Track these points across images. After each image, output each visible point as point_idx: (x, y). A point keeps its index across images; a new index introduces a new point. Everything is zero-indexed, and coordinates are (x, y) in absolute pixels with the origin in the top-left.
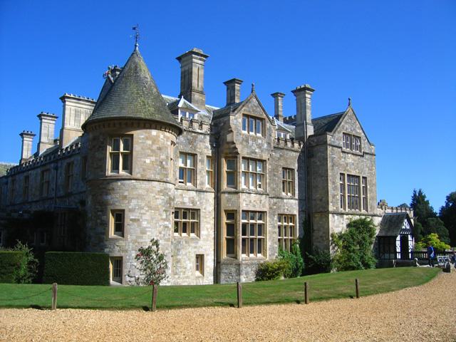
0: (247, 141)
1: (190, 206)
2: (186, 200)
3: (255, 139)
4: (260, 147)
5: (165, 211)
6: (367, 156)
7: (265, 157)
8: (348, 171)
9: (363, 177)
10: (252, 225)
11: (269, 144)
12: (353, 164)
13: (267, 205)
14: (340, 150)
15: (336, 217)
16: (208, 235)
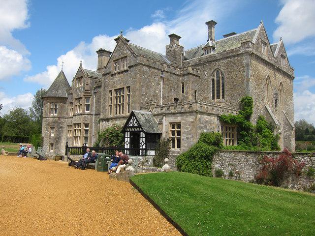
4: (80, 91)
9: (127, 87)
10: (78, 130)
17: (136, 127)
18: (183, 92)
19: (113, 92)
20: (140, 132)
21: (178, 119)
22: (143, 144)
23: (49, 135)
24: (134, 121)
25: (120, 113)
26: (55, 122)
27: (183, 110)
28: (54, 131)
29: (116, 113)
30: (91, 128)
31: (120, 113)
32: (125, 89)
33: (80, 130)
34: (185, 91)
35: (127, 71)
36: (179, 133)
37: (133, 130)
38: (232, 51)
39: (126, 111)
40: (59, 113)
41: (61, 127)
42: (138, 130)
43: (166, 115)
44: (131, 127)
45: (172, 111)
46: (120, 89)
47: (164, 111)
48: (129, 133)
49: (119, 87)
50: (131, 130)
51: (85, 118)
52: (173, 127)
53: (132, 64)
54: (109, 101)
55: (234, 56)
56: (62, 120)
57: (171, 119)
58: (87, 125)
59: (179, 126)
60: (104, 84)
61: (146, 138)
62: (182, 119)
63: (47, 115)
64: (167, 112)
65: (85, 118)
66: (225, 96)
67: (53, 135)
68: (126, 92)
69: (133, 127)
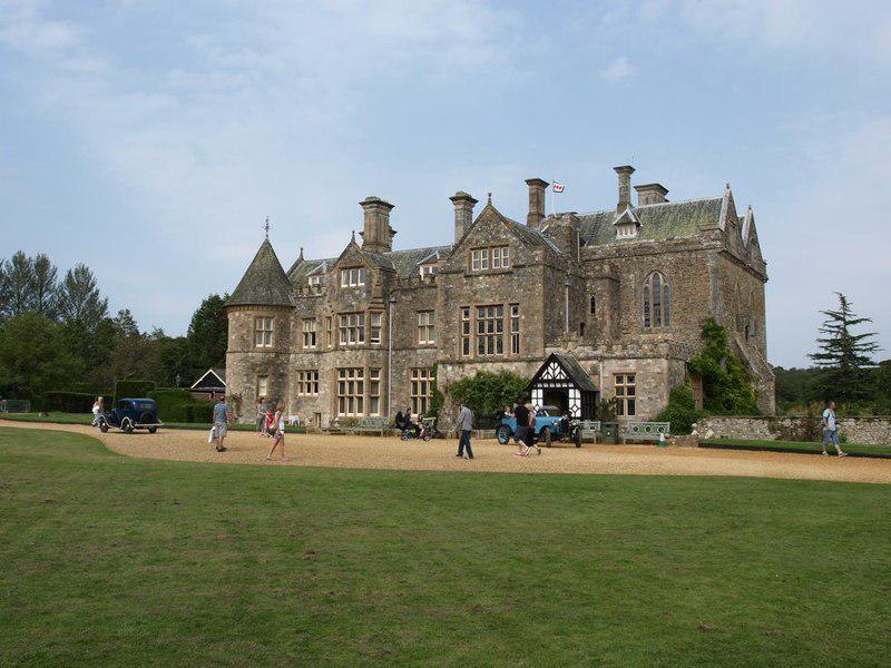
0: (342, 295)
1: (310, 367)
2: (306, 362)
3: (351, 291)
4: (356, 298)
5: (247, 375)
6: (521, 271)
7: (364, 307)
8: (476, 301)
10: (351, 383)
11: (369, 292)
12: (488, 289)
13: (364, 360)
14: (462, 275)
15: (450, 368)
16: (326, 394)
17: (561, 381)
18: (593, 311)
19: (472, 312)
20: (568, 389)
21: (632, 365)
22: (575, 409)
23: (254, 392)
24: (554, 370)
25: (491, 351)
26: (270, 362)
27: (639, 354)
28: (264, 383)
29: (482, 352)
30: (386, 376)
31: (491, 351)
32: (505, 308)
33: (360, 383)
34: (597, 310)
35: (510, 273)
36: (631, 391)
37: (552, 386)
38: (685, 242)
39: (509, 349)
40: (277, 342)
41: (282, 375)
42: (565, 385)
43: (602, 359)
44: (548, 381)
45: (618, 354)
46: (491, 307)
47: (599, 352)
48: (541, 392)
49: (489, 301)
50: (546, 386)
51: (372, 356)
52: (620, 379)
53: (520, 263)
54: (460, 328)
55: (690, 251)
56: (282, 358)
57: (614, 366)
58: (374, 372)
59: (631, 379)
60: (446, 292)
61: (582, 399)
62: (639, 367)
63: (248, 346)
64: (606, 355)
65: (372, 356)
66: (672, 323)
67: (263, 393)
68: (508, 314)
69: (554, 380)
